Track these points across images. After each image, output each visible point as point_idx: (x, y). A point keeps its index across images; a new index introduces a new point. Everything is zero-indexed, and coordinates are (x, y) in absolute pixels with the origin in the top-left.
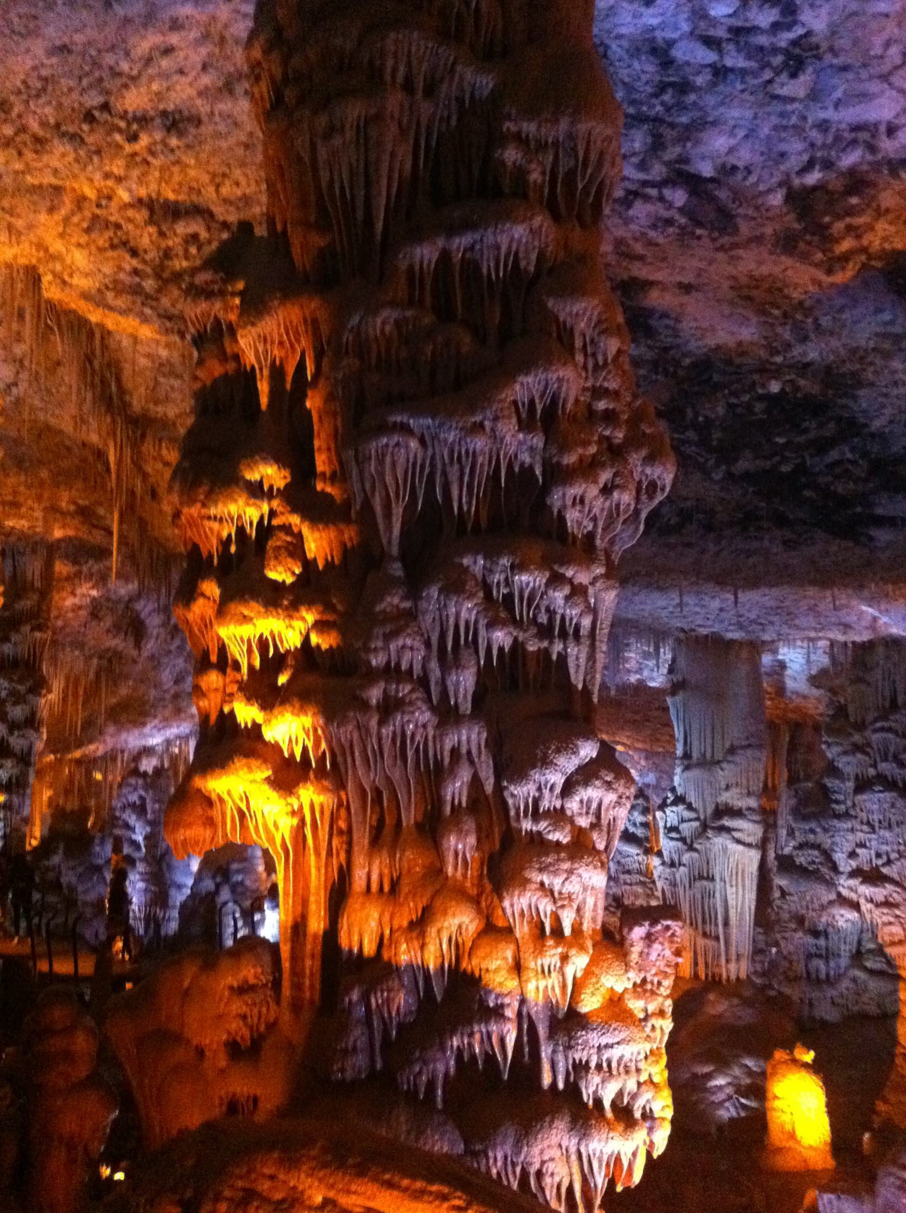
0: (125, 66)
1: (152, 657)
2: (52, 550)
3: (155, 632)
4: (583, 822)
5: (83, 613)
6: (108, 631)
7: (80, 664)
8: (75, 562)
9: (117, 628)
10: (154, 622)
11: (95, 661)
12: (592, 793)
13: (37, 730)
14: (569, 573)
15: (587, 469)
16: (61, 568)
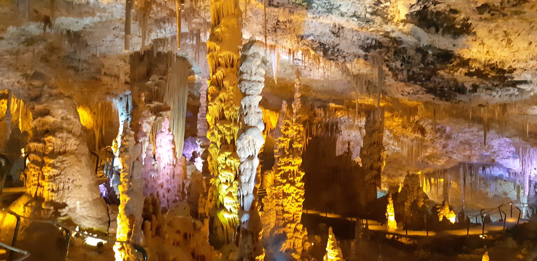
0: (275, 14)
1: (431, 140)
2: (383, 109)
3: (429, 132)
4: (229, 165)
5: (400, 127)
6: (411, 132)
7: (410, 143)
8: (391, 112)
9: (414, 131)
10: (428, 128)
11: (415, 141)
12: (228, 160)
13: (382, 161)
14: (225, 125)
15: (228, 109)
16: (387, 114)
